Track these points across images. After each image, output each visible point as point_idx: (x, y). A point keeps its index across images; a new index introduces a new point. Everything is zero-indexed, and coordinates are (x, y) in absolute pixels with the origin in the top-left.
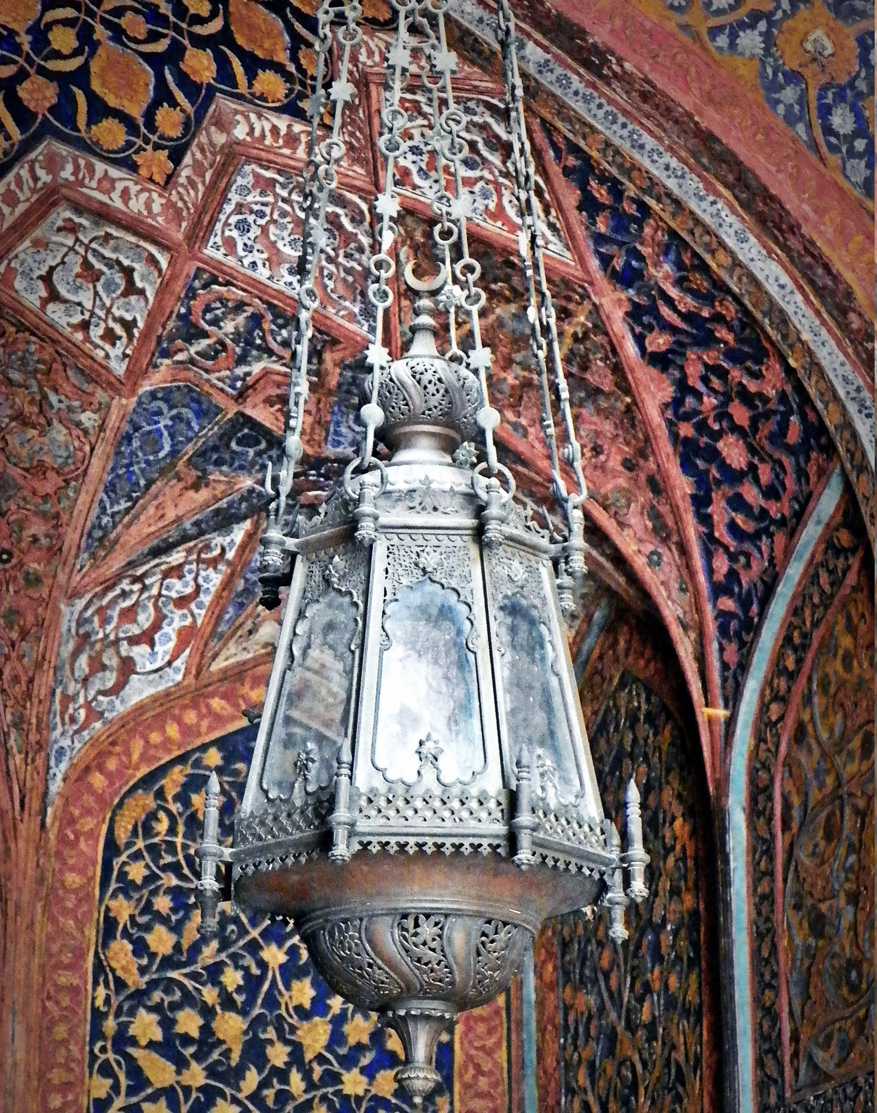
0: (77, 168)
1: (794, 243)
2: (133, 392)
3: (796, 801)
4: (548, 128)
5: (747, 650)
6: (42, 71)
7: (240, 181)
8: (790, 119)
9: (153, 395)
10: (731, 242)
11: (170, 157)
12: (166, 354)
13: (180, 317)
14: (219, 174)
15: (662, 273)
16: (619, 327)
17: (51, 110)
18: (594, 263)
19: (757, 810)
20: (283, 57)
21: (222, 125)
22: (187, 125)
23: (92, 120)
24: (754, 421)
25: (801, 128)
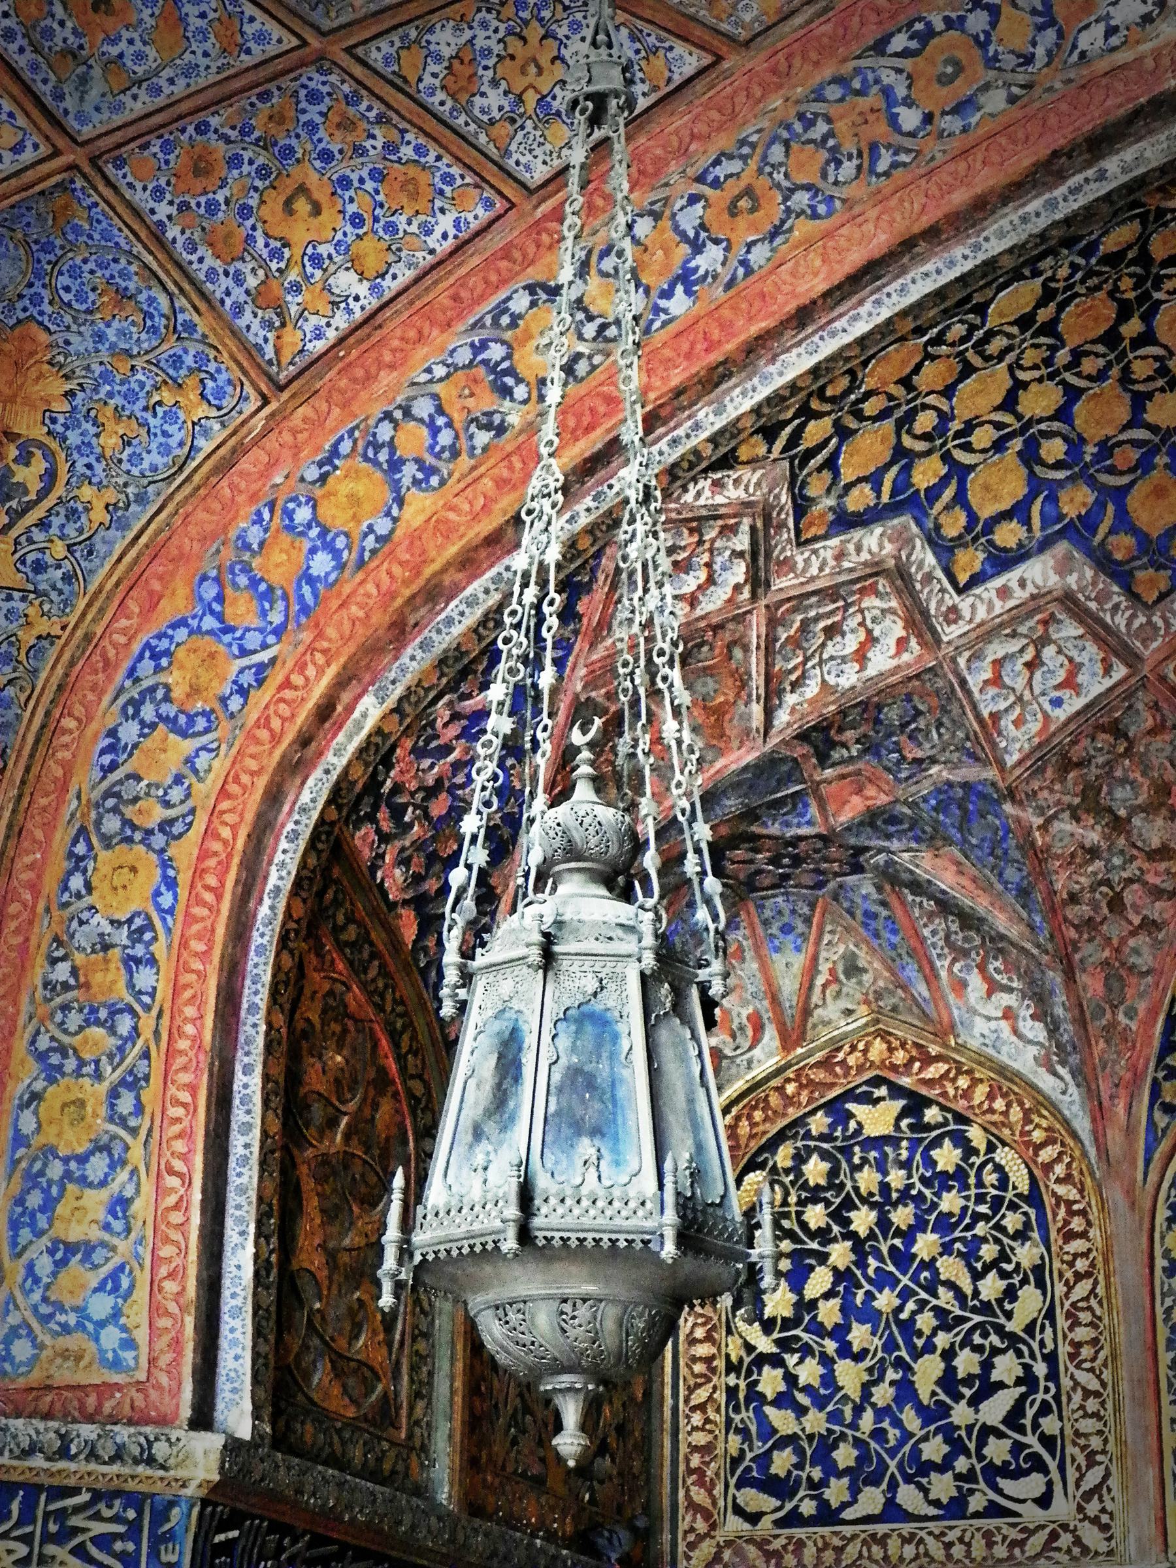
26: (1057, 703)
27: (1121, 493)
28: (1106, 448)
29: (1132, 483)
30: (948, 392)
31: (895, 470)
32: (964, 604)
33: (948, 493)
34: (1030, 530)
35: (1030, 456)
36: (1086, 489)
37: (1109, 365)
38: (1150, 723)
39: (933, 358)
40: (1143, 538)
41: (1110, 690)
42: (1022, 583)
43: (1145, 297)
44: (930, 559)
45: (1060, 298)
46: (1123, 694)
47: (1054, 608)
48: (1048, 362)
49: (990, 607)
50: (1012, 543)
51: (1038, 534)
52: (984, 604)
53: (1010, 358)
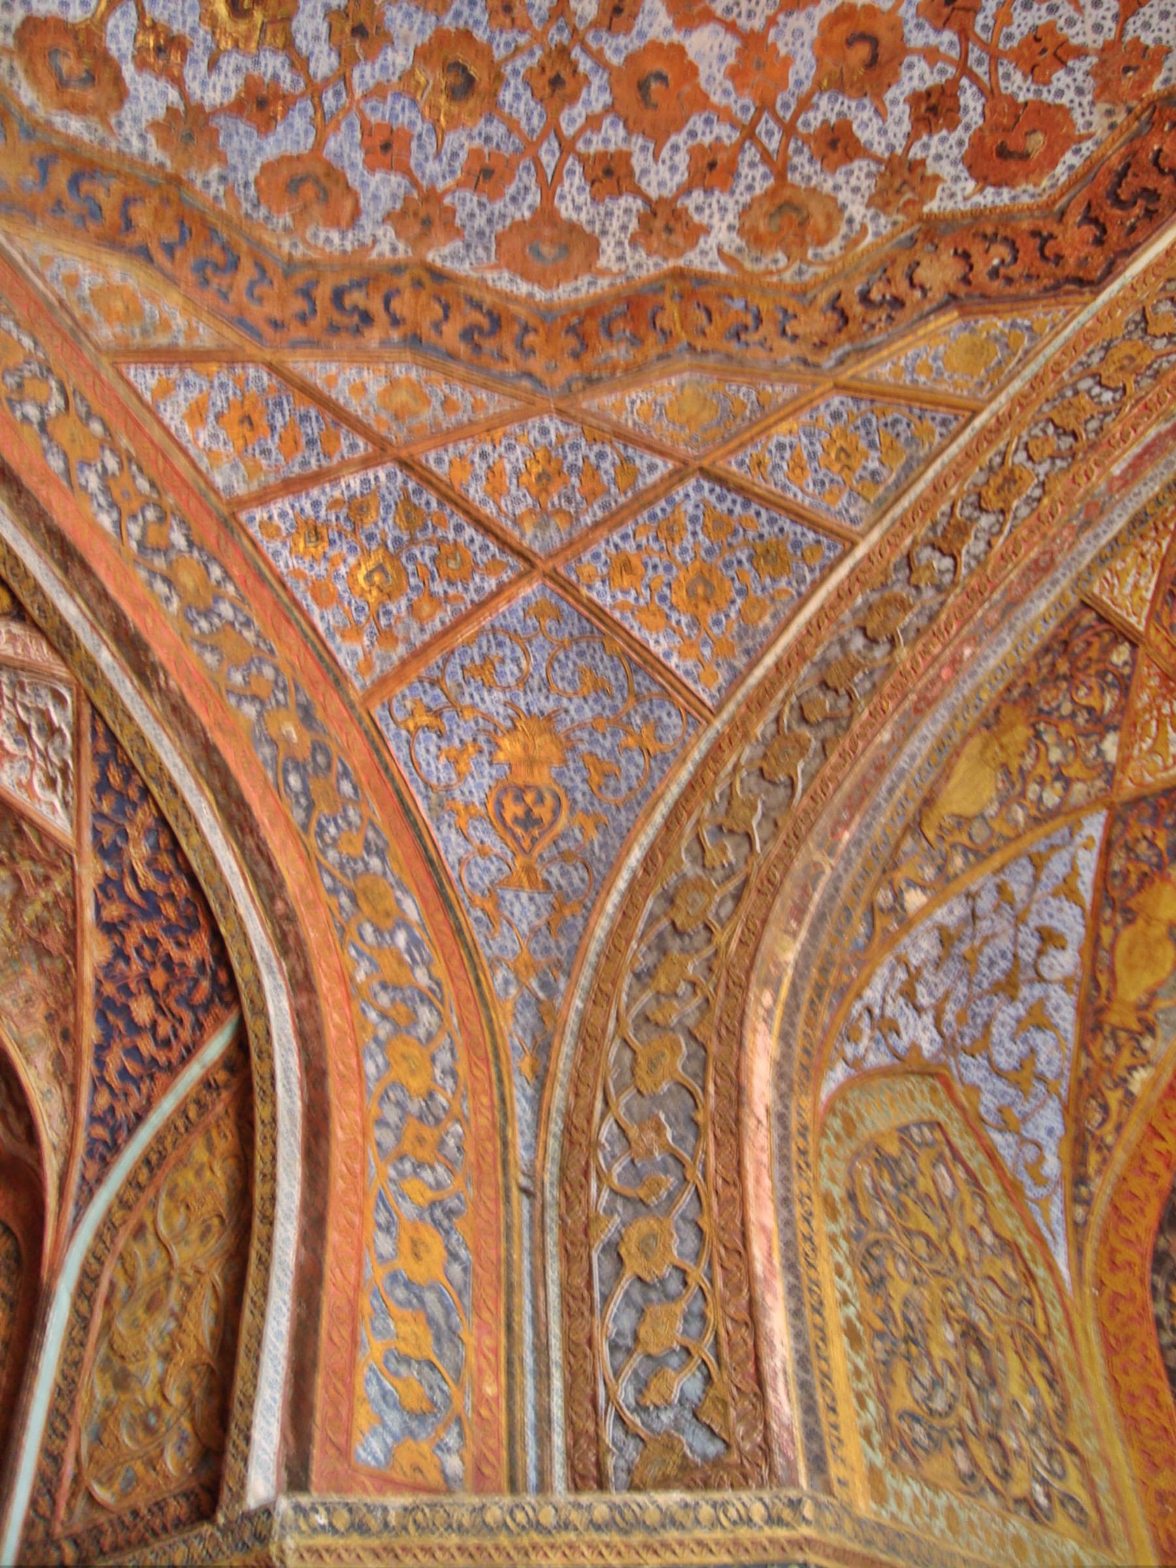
1: (250, 842)
3: (122, 1285)
4: (96, 712)
5: (106, 1164)
8: (265, 762)
10: (205, 828)
15: (138, 852)
16: (87, 895)
18: (87, 836)
19: (85, 1290)
24: (167, 988)
25: (270, 775)
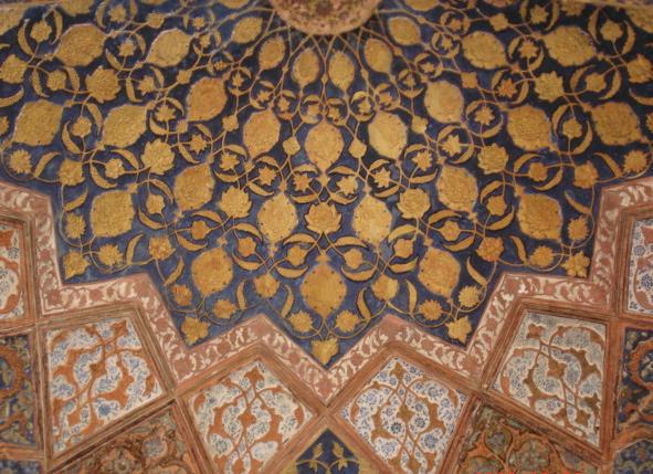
0: (528, 285)
2: (609, 458)
6: (491, 234)
7: (636, 243)
9: (623, 455)
11: (585, 255)
12: (623, 419)
13: (626, 381)
14: (620, 241)
17: (501, 256)
20: (636, 135)
21: (611, 206)
22: (589, 225)
23: (529, 253)
26: (105, 410)
27: (191, 256)
28: (191, 217)
29: (199, 251)
30: (106, 107)
31: (50, 156)
32: (66, 293)
33: (81, 200)
34: (125, 257)
35: (139, 203)
36: (167, 243)
37: (208, 149)
38: (163, 454)
39: (108, 66)
40: (196, 294)
41: (147, 406)
42: (110, 292)
43: (244, 99)
44: (52, 243)
45: (195, 68)
46: (152, 413)
47: (127, 317)
48: (173, 123)
49: (83, 301)
50: (110, 262)
51: (129, 262)
52: (80, 298)
53: (151, 105)
